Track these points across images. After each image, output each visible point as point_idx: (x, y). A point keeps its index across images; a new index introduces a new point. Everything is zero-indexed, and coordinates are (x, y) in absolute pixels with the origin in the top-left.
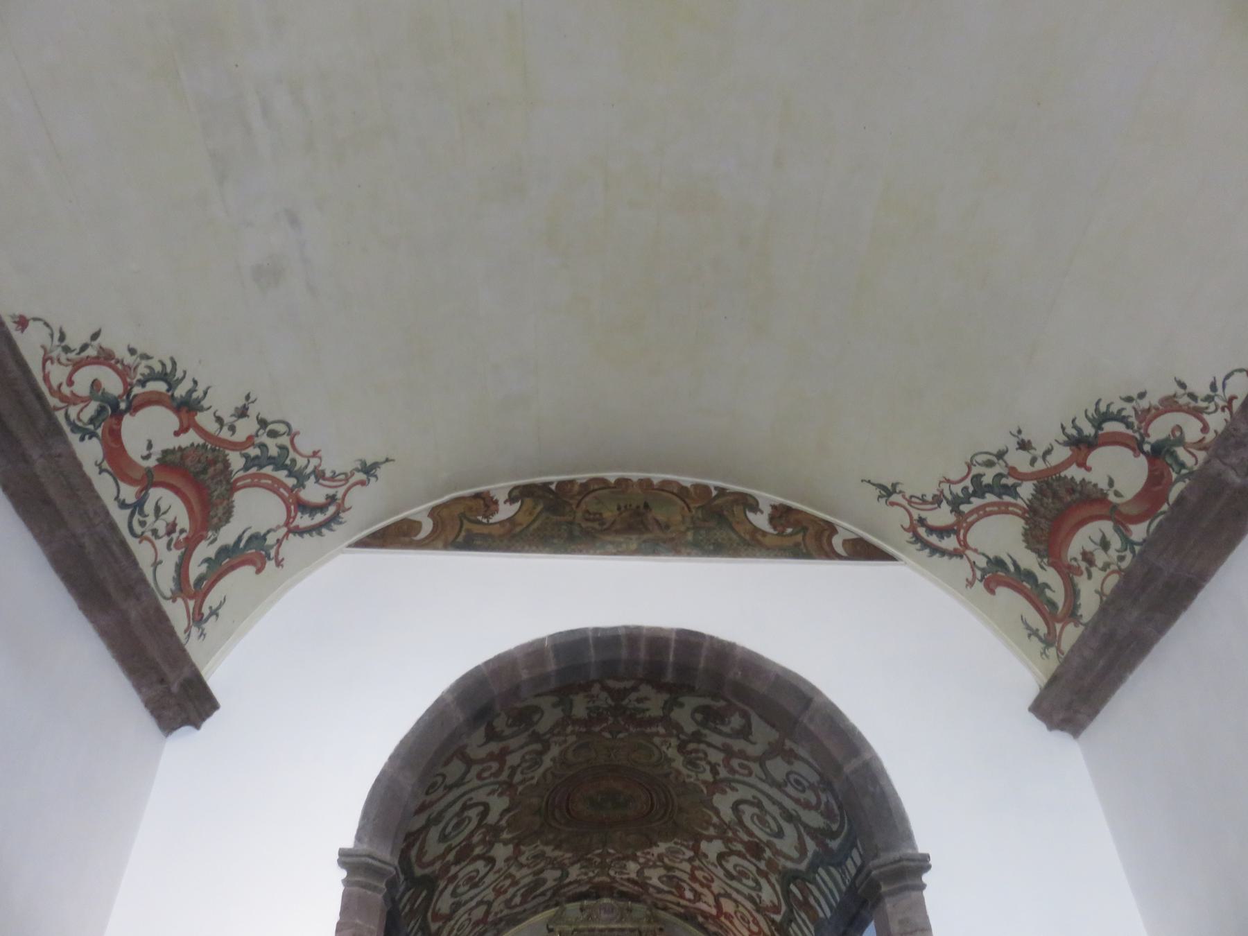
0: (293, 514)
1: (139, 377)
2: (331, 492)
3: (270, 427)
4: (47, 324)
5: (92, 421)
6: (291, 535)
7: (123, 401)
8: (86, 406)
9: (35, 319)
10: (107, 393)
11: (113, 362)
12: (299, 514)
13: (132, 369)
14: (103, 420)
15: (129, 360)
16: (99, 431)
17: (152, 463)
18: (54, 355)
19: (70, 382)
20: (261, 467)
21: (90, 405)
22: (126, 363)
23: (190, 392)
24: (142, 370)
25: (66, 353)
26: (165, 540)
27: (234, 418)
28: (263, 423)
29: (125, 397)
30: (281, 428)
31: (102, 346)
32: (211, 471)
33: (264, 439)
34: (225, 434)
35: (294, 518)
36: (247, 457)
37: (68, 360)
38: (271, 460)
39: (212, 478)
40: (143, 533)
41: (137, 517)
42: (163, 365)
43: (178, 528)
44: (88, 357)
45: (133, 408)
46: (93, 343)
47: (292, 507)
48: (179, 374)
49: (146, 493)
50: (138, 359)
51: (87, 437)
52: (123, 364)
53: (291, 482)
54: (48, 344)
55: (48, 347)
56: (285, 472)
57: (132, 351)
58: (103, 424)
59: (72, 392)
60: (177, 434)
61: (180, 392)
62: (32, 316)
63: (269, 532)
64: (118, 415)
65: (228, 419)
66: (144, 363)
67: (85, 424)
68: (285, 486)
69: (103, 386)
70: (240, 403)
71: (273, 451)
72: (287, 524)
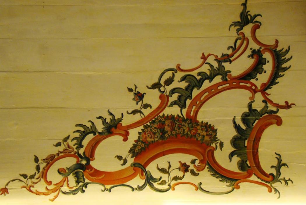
0: (249, 85)
1: (75, 147)
2: (248, 52)
3: (162, 82)
4: (13, 180)
5: (78, 182)
6: (268, 91)
7: (81, 161)
8: (68, 181)
9: (7, 185)
10: (70, 168)
11: (56, 157)
12: (253, 81)
13: (68, 148)
14: (83, 176)
15: (61, 148)
16: (87, 181)
17: (131, 161)
18: (30, 184)
19: (50, 183)
20: (190, 96)
21: (69, 179)
22: (61, 150)
23: (104, 121)
24: (72, 143)
25: (34, 178)
26: (188, 174)
27: (140, 103)
28: (156, 86)
29: (80, 159)
30: (169, 74)
31: (44, 158)
32: (167, 128)
33: (169, 88)
34: (147, 112)
35: (253, 84)
36: (175, 103)
37: (37, 179)
38: (190, 89)
39: (173, 129)
40: (169, 185)
41: (156, 185)
42: (77, 131)
43: (188, 163)
44: (44, 168)
45: (90, 156)
46: (39, 163)
47: (241, 84)
48: (89, 125)
49: (146, 172)
50: (65, 143)
51: (84, 188)
52: (61, 152)
53: (218, 79)
54: (23, 184)
55: (24, 184)
56: (207, 82)
57: (59, 144)
58: (85, 177)
59: (55, 185)
60: (125, 140)
61: (100, 127)
62: (5, 185)
63: (250, 106)
64: (87, 166)
65: (138, 107)
66: (69, 141)
67: (76, 187)
68: (219, 84)
69: (65, 167)
70: (132, 96)
71: (184, 85)
72: (255, 91)
